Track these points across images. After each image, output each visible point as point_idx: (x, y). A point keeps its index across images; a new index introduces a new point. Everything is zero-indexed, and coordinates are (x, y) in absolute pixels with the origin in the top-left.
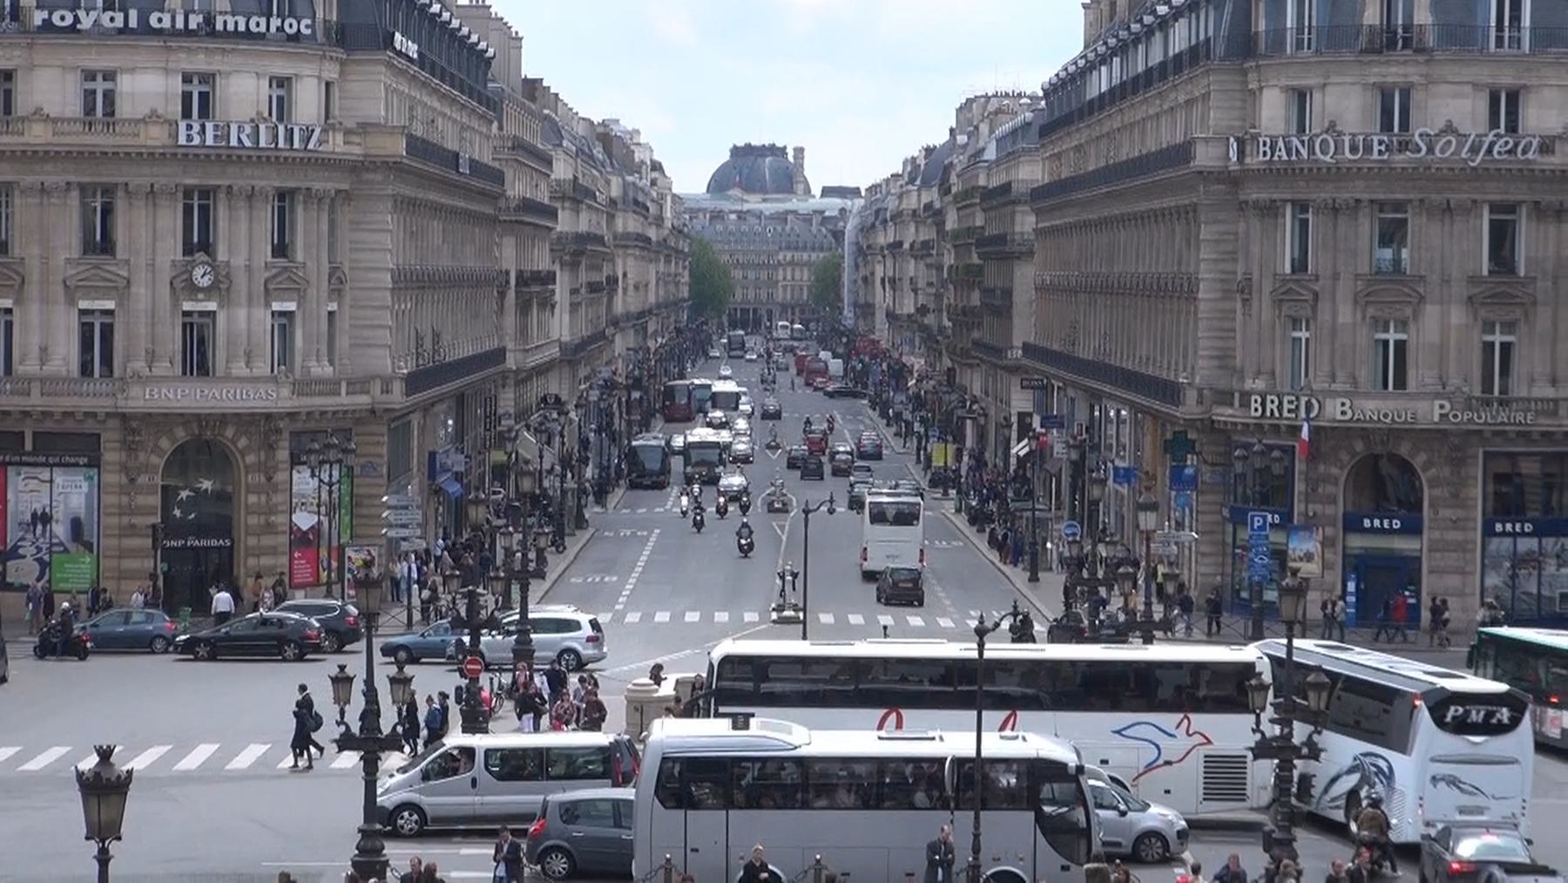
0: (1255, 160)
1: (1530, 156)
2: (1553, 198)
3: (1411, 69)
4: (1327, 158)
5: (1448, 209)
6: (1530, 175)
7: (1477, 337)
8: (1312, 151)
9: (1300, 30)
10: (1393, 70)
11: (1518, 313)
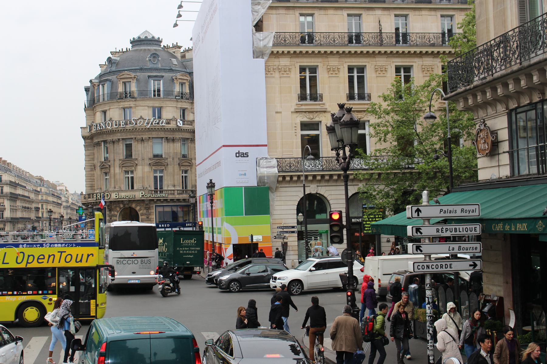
0: (94, 131)
1: (163, 124)
2: (171, 136)
3: (131, 103)
4: (109, 128)
5: (142, 140)
6: (163, 130)
7: (152, 175)
8: (106, 126)
9: (104, 95)
10: (126, 103)
11: (163, 168)
